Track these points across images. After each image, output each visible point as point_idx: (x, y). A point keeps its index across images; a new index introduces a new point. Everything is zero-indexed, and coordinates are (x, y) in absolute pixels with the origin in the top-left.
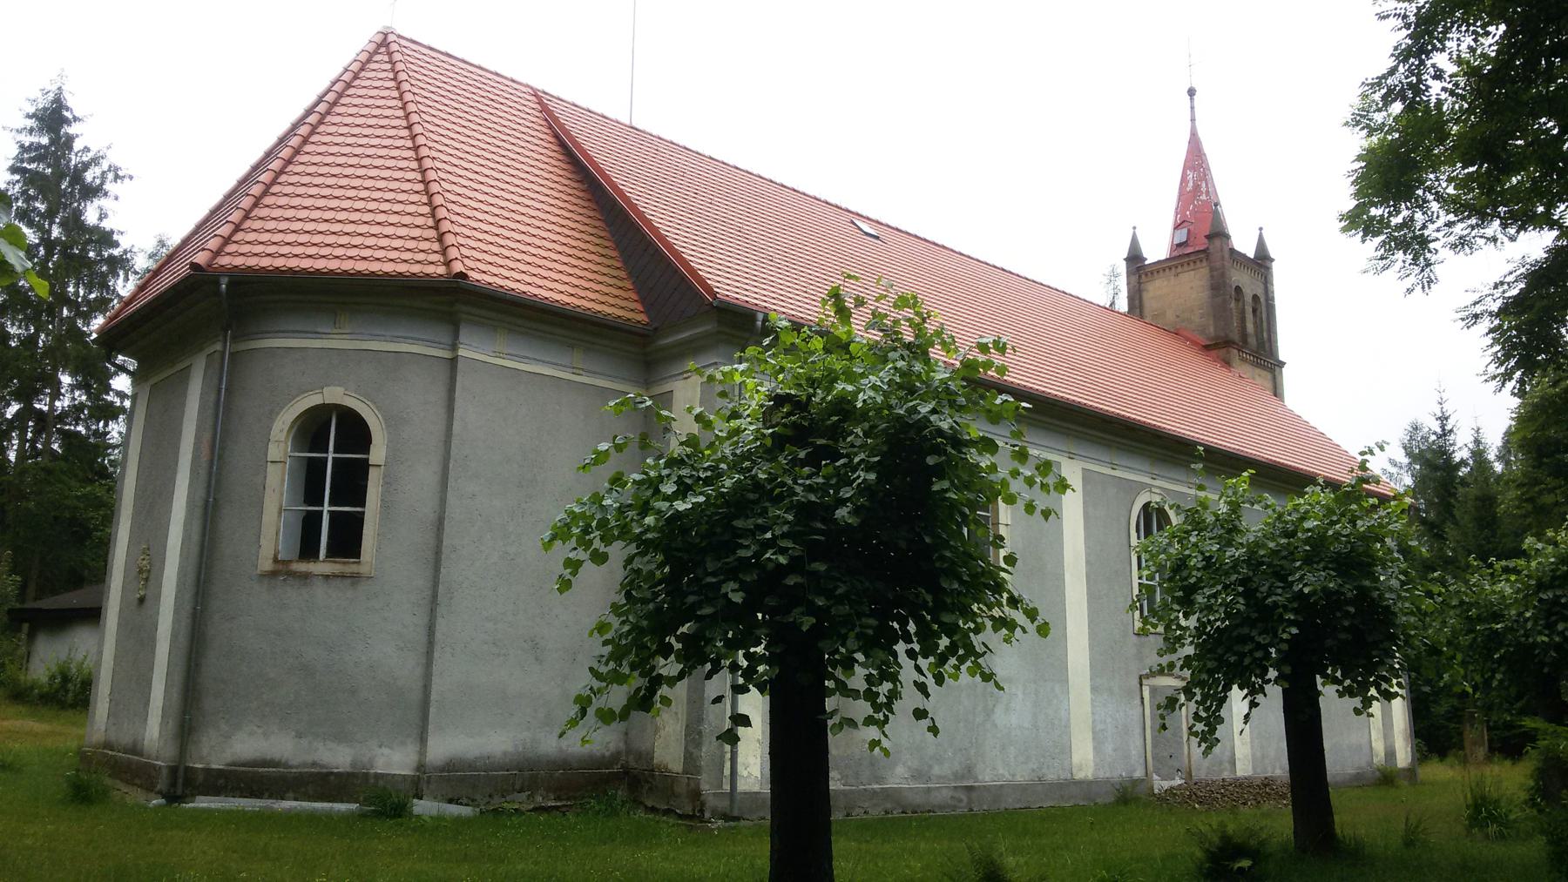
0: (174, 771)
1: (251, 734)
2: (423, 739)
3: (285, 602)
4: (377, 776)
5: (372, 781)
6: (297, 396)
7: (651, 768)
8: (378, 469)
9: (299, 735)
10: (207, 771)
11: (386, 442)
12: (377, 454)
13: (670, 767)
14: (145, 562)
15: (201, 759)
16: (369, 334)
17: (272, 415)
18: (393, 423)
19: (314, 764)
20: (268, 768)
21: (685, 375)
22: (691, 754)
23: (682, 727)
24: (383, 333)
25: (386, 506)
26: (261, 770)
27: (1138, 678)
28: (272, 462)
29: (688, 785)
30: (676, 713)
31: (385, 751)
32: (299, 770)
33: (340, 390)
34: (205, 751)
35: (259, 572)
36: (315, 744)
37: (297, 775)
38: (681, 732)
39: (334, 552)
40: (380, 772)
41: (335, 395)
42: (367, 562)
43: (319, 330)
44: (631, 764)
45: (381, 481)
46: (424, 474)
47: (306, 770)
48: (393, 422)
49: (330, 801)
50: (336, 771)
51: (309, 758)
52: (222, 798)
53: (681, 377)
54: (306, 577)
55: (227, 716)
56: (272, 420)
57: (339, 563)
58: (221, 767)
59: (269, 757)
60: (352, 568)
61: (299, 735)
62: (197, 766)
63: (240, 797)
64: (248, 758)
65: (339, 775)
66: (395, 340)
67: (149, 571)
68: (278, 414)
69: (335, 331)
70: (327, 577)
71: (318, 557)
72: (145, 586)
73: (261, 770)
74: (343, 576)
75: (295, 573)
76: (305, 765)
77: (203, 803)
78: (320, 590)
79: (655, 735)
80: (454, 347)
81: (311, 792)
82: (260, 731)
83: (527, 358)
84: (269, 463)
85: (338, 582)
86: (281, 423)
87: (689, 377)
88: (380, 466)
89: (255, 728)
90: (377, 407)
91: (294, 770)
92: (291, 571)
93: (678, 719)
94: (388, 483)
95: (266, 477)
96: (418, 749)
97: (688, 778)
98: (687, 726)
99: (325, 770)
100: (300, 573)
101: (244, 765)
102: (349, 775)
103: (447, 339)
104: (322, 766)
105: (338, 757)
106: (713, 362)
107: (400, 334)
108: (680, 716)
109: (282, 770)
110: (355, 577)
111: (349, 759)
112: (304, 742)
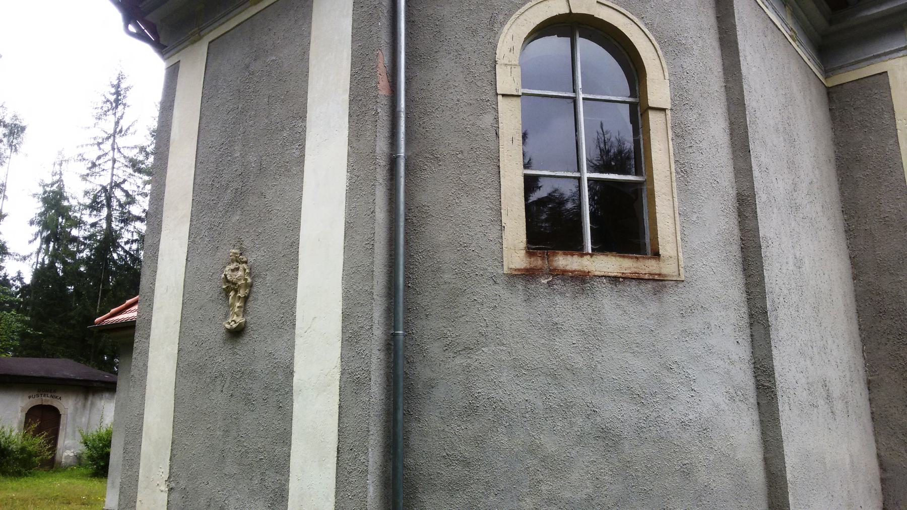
3: (556, 320)
14: (240, 273)
17: (494, 25)
28: (503, 95)
35: (506, 271)
39: (603, 245)
54: (582, 279)
56: (496, 34)
60: (648, 266)
67: (250, 286)
68: (502, 24)
70: (614, 280)
72: (244, 311)
74: (638, 279)
75: (564, 272)
84: (500, 97)
85: (633, 288)
86: (509, 37)
88: (664, 110)
90: (646, 24)
92: (555, 270)
95: (496, 119)
100: (572, 272)
110: (658, 282)
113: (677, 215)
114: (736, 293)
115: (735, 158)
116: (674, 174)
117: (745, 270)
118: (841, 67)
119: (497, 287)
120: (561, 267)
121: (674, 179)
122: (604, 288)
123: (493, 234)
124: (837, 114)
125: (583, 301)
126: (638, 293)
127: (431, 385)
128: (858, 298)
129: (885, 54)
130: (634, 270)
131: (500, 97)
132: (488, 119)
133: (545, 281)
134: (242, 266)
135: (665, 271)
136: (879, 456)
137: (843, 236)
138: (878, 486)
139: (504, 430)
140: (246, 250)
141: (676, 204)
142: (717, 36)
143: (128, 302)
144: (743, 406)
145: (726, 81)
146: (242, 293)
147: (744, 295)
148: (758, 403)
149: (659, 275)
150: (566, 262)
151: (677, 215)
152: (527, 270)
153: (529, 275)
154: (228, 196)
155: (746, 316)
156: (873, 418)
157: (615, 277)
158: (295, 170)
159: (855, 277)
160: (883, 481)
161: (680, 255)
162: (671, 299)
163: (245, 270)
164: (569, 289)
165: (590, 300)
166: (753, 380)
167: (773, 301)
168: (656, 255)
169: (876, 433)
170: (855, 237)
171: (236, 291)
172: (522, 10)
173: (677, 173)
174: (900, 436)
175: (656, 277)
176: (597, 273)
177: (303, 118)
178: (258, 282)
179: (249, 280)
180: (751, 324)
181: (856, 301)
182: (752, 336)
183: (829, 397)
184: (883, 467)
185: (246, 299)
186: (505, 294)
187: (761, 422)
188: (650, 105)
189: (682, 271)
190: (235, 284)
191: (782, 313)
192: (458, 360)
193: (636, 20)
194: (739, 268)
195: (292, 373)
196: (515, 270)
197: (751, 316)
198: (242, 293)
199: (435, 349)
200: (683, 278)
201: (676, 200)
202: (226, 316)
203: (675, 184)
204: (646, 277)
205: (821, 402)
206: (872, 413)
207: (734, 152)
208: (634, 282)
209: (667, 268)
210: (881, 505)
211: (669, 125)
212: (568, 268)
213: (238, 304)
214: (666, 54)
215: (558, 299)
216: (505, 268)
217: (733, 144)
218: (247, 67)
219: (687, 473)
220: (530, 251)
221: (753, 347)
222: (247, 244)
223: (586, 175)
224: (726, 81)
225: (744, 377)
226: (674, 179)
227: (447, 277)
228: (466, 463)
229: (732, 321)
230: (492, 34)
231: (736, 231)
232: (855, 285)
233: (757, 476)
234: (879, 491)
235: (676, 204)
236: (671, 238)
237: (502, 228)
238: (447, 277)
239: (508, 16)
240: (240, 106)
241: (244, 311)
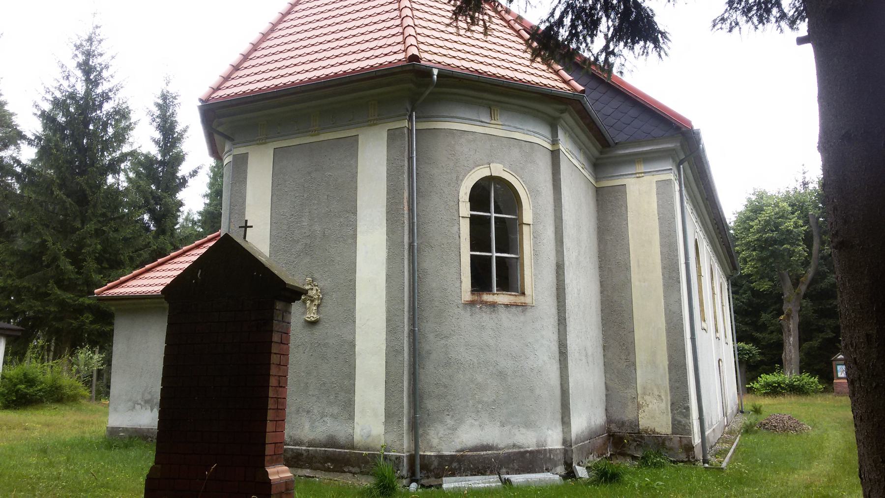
0: (412, 458)
1: (472, 425)
2: (565, 420)
3: (483, 324)
4: (551, 451)
5: (548, 455)
6: (474, 168)
7: (637, 431)
8: (528, 226)
9: (503, 425)
10: (441, 457)
11: (531, 208)
12: (527, 216)
13: (657, 430)
15: (431, 448)
16: (514, 127)
18: (534, 193)
19: (514, 446)
20: (486, 451)
21: (638, 175)
22: (680, 422)
23: (667, 405)
24: (521, 127)
25: (536, 254)
26: (482, 453)
27: (718, 360)
28: (462, 217)
29: (681, 442)
30: (660, 396)
31: (550, 432)
32: (506, 451)
33: (500, 166)
34: (435, 441)
36: (513, 431)
37: (506, 455)
38: (667, 409)
40: (550, 448)
41: (498, 170)
42: (529, 295)
43: (483, 120)
44: (613, 429)
45: (532, 236)
46: (549, 233)
47: (510, 451)
48: (534, 193)
49: (529, 473)
50: (529, 449)
51: (510, 442)
52: (458, 478)
53: (633, 176)
54: (493, 305)
55: (451, 413)
56: (459, 186)
57: (513, 295)
58: (454, 453)
59: (485, 443)
60: (521, 299)
61: (503, 425)
62: (428, 453)
63: (471, 475)
64: (471, 445)
65: (531, 452)
66: (529, 133)
68: (462, 181)
69: (493, 122)
70: (507, 306)
71: (491, 291)
73: (482, 453)
74: (516, 305)
75: (486, 302)
76: (508, 447)
77: (449, 484)
78: (504, 316)
79: (638, 410)
80: (555, 142)
81: (517, 467)
82: (477, 423)
83: (573, 154)
84: (461, 218)
85: (513, 309)
87: (643, 176)
88: (529, 225)
89: (473, 421)
90: (523, 181)
91: (501, 452)
92: (483, 301)
93: (662, 400)
94: (536, 236)
95: (459, 229)
96: (562, 430)
97: (680, 437)
98: (672, 404)
99: (522, 450)
100: (490, 302)
101: (471, 450)
102: (538, 452)
103: (548, 134)
104: (519, 447)
105: (527, 440)
106: (668, 168)
107: (532, 130)
108: (663, 397)
109: (495, 452)
110: (524, 306)
111: (535, 440)
112: (506, 428)
113: (533, 275)
114: (554, 311)
115: (557, 245)
116: (532, 256)
117: (557, 299)
118: (604, 177)
119: (459, 309)
120: (485, 300)
121: (532, 258)
122: (502, 309)
123: (458, 285)
124: (600, 203)
125: (494, 316)
126: (516, 312)
127: (429, 353)
128: (602, 303)
129: (626, 175)
130: (514, 301)
131: (461, 218)
132: (456, 228)
133: (479, 307)
134: (315, 288)
135: (527, 302)
136: (606, 383)
137: (597, 270)
138: (604, 398)
139: (461, 372)
140: (316, 279)
141: (533, 271)
142: (552, 183)
143: (122, 279)
144: (554, 361)
145: (555, 206)
146: (316, 302)
147: (557, 311)
148: (560, 360)
149: (525, 303)
150: (487, 297)
151: (533, 275)
152: (471, 301)
153: (472, 303)
154: (299, 247)
155: (557, 320)
156: (604, 365)
157: (507, 304)
158: (350, 241)
159: (602, 292)
160: (606, 395)
161: (534, 294)
162: (529, 313)
163: (317, 290)
164: (488, 310)
165: (497, 315)
166: (558, 349)
167: (568, 314)
168: (523, 294)
169: (605, 372)
170: (603, 271)
171: (312, 301)
172: (470, 174)
173: (534, 255)
174: (616, 373)
175: (523, 304)
176: (500, 303)
177: (355, 213)
178: (326, 297)
179: (321, 296)
180: (559, 324)
181: (602, 304)
182: (559, 329)
183: (586, 356)
184: (607, 388)
185: (318, 306)
186: (462, 312)
187: (560, 368)
188: (524, 222)
189: (534, 301)
190: (312, 297)
191: (571, 319)
192: (442, 342)
193: (519, 179)
194: (555, 298)
195: (354, 346)
196: (467, 301)
197: (559, 320)
198: (316, 302)
199: (431, 337)
200: (534, 305)
201: (533, 268)
202: (304, 313)
203: (532, 261)
204: (519, 304)
205: (584, 358)
206: (604, 362)
207: (556, 242)
208: (514, 307)
209: (527, 300)
210: (605, 407)
211: (531, 232)
212: (488, 300)
213: (314, 308)
214: (531, 196)
215: (484, 314)
216: (463, 301)
217: (556, 238)
218: (309, 173)
219: (532, 390)
220: (473, 291)
221: (559, 334)
222: (316, 276)
223: (495, 255)
224: (555, 206)
225: (555, 348)
226: (532, 258)
227: (437, 304)
228: (445, 387)
229: (552, 323)
230: (457, 186)
231: (555, 280)
232: (601, 296)
233: (558, 392)
234: (605, 400)
235: (533, 271)
236: (530, 287)
237: (461, 282)
238: (437, 304)
239: (465, 176)
240: (305, 196)
241: (318, 312)
